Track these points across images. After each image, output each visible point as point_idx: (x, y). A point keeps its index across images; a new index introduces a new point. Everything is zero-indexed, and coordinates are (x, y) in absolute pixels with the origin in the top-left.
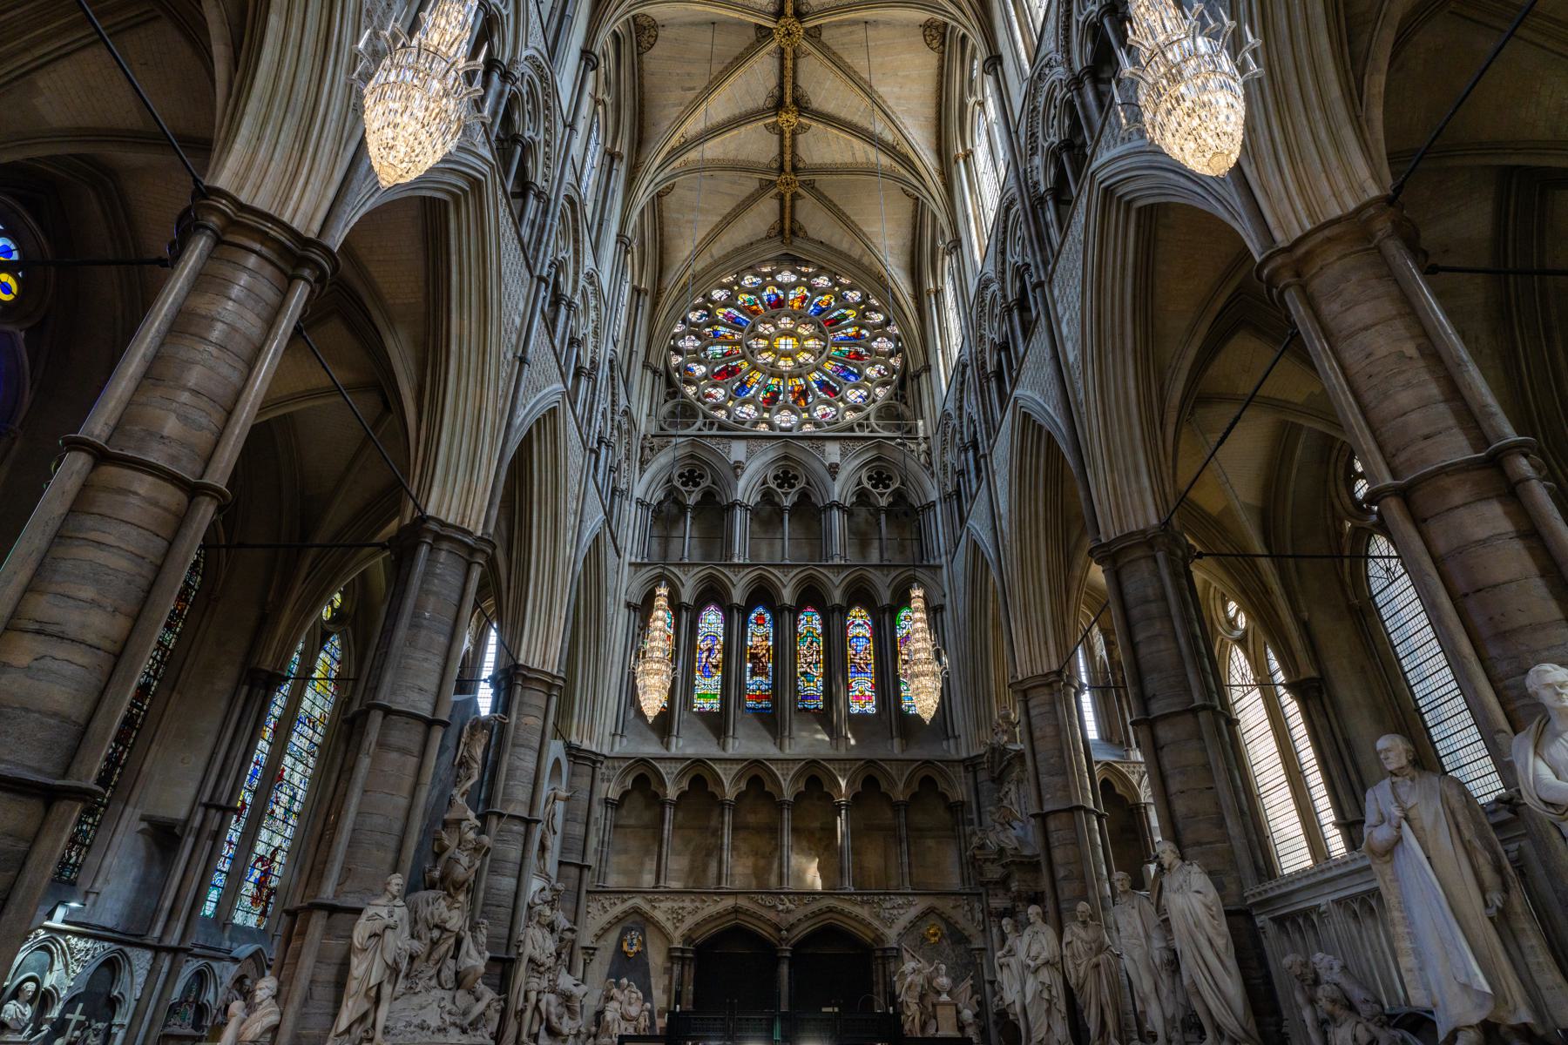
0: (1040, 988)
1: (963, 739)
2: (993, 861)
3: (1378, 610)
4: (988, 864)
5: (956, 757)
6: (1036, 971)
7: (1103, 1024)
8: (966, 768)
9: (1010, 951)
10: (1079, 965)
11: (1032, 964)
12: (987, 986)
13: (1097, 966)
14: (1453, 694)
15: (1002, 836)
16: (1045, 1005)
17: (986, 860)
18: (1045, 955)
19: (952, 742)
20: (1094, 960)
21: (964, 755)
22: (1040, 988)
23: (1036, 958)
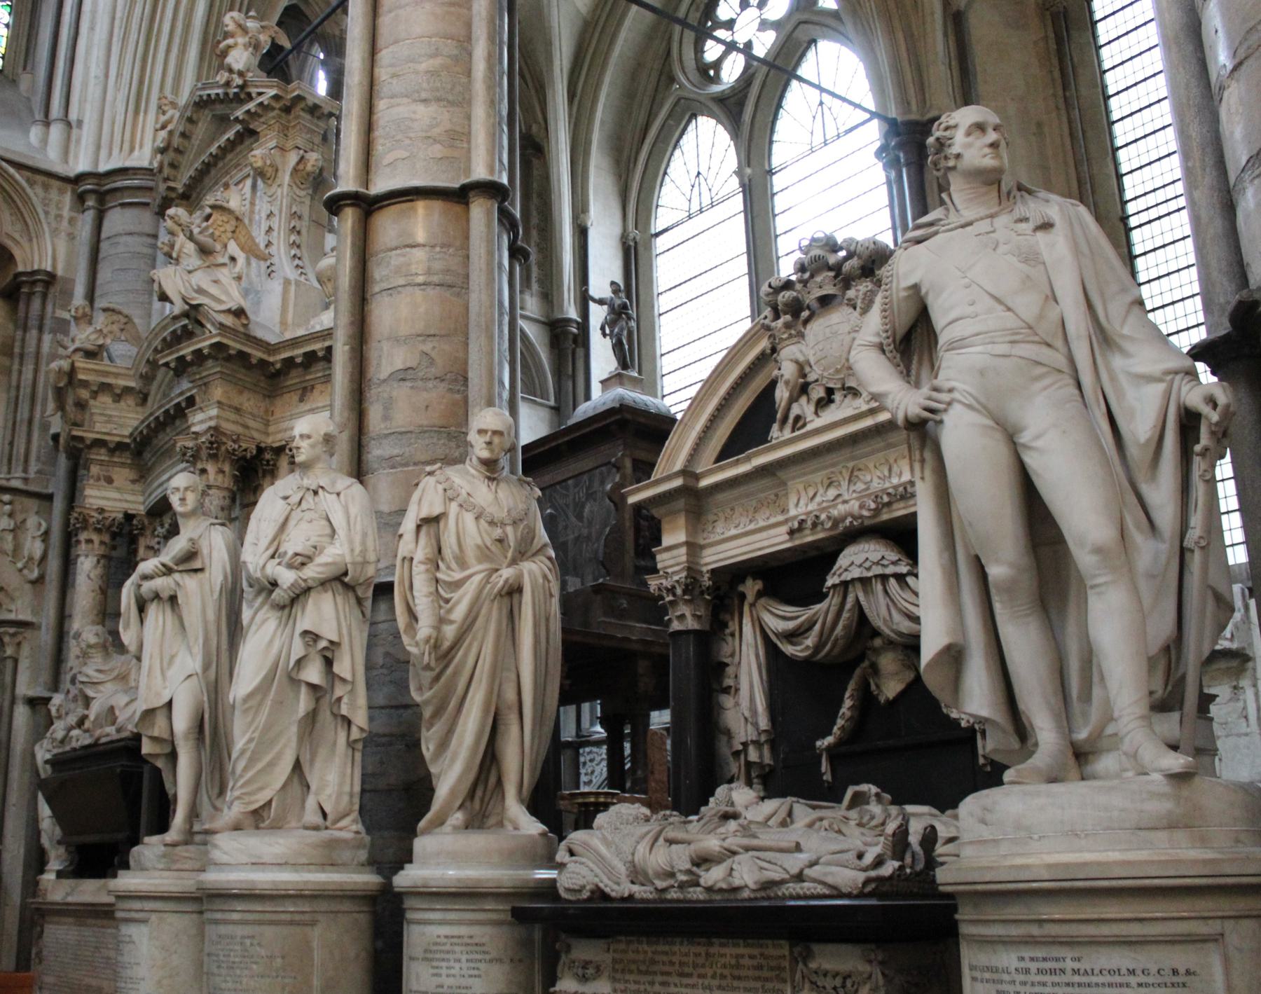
0: (298, 649)
1: (87, 135)
2: (119, 395)
3: (1094, 24)
4: (105, 399)
5: (59, 169)
6: (300, 595)
7: (490, 758)
8: (81, 198)
9: (191, 555)
10: (457, 585)
11: (287, 577)
12: (21, 714)
13: (513, 591)
14: (1173, 206)
15: (200, 279)
16: (304, 703)
17: (105, 387)
18: (335, 554)
19: (56, 131)
20: (507, 573)
21: (81, 165)
22: (298, 649)
23: (300, 561)
